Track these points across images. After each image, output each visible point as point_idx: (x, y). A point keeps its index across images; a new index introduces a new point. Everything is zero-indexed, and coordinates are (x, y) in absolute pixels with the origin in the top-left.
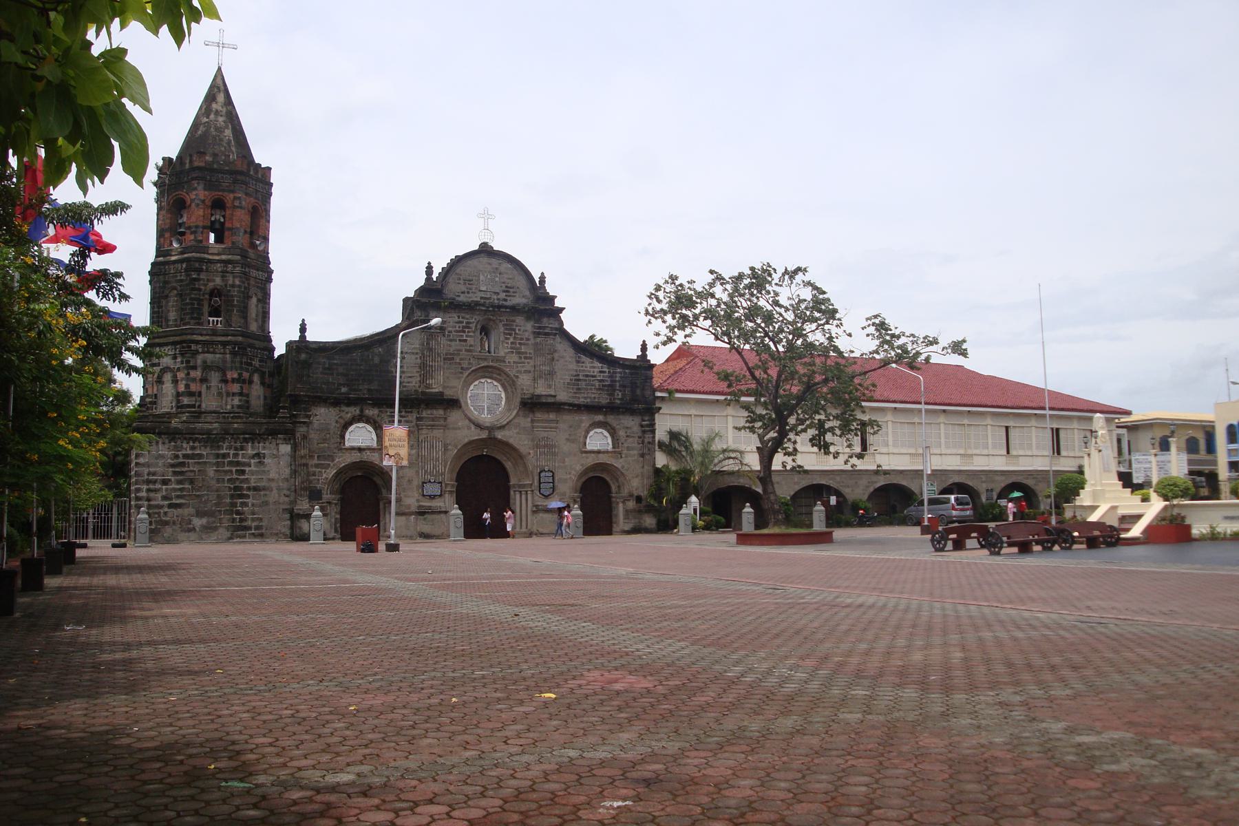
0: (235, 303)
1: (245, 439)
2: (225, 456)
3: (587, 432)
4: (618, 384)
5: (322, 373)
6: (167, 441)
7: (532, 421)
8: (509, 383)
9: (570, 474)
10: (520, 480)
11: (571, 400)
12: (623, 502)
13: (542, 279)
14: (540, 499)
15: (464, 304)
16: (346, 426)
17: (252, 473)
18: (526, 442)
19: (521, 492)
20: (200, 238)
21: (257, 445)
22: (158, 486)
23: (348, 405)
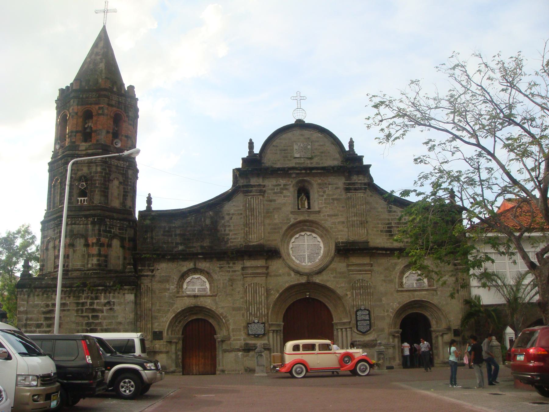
0: (97, 185)
1: (98, 290)
2: (83, 304)
3: (403, 273)
5: (163, 235)
6: (41, 294)
7: (348, 266)
8: (324, 232)
9: (387, 311)
10: (341, 319)
13: (351, 144)
14: (358, 336)
15: (279, 169)
16: (183, 276)
18: (343, 285)
19: (342, 329)
20: (74, 140)
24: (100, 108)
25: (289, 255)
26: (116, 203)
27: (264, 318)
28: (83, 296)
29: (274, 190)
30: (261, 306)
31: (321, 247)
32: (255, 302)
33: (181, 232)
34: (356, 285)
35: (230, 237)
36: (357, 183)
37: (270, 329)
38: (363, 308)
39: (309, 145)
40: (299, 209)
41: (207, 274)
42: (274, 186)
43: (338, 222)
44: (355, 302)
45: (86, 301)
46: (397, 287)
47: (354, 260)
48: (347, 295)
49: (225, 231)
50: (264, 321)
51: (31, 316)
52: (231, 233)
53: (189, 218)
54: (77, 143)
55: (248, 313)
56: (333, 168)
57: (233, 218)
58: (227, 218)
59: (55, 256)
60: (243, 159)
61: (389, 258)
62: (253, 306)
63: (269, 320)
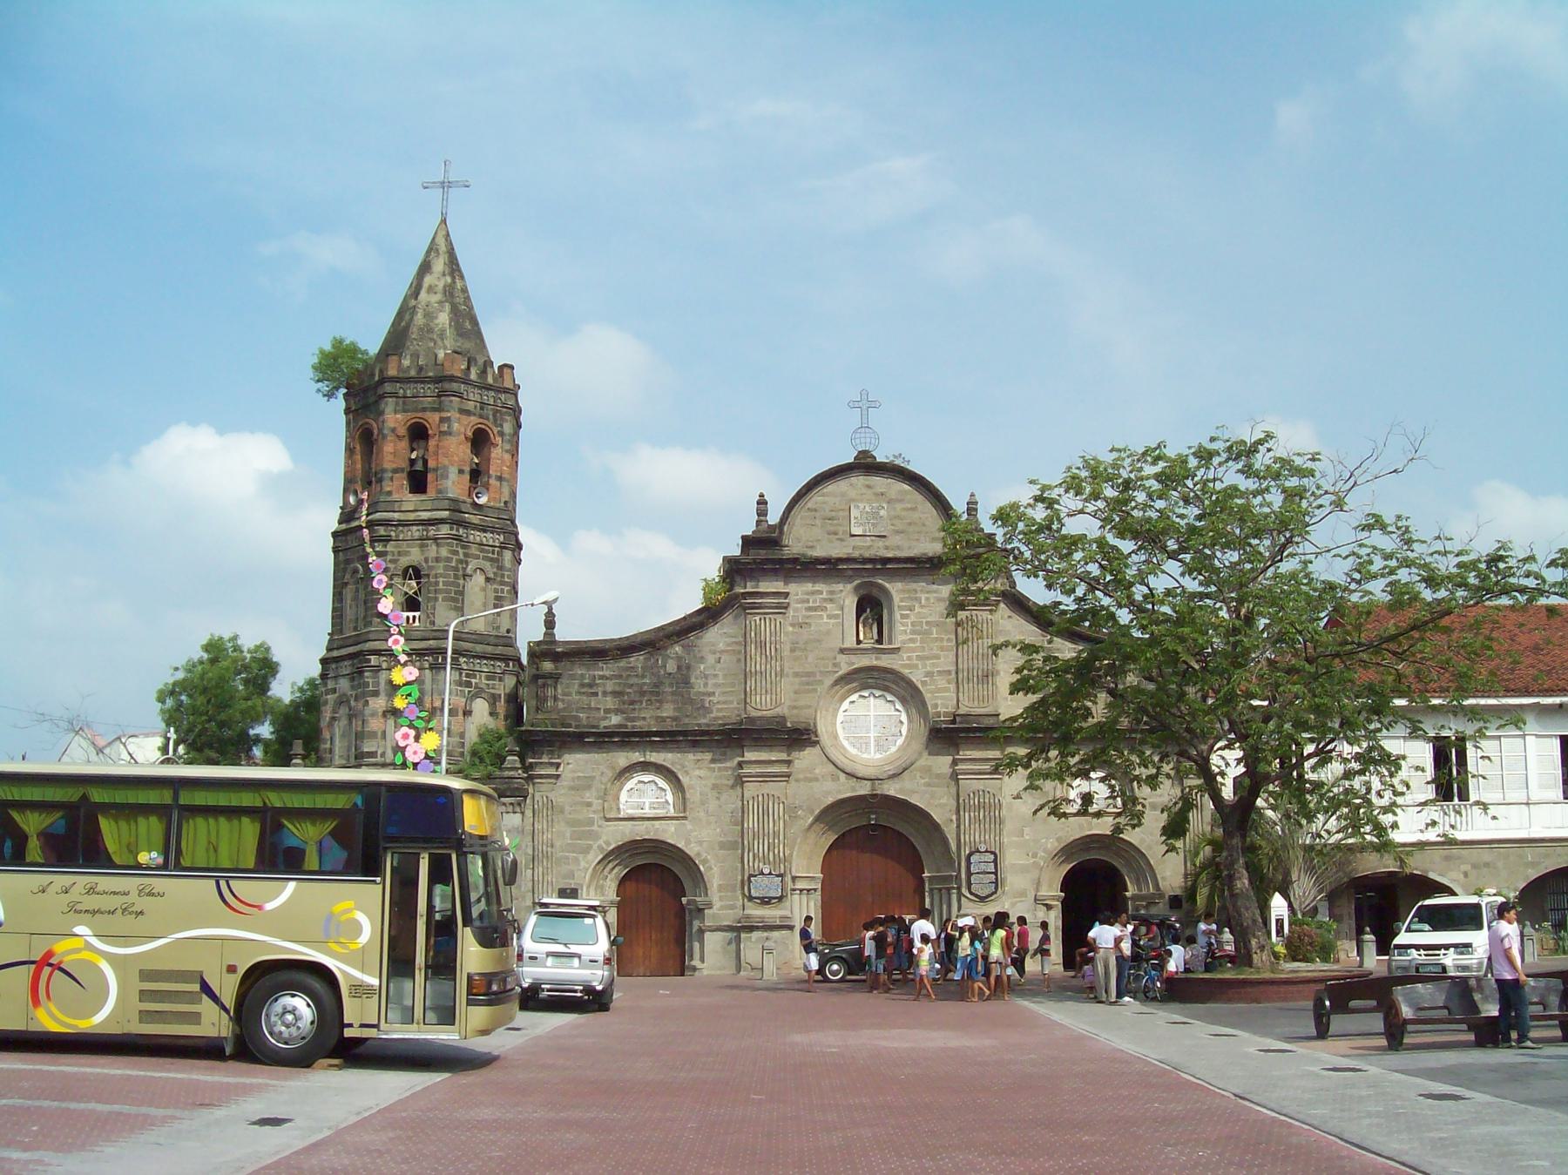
0: (441, 586)
7: (955, 762)
9: (1035, 855)
13: (972, 508)
18: (944, 801)
25: (836, 737)
29: (808, 602)
31: (901, 722)
33: (617, 689)
35: (715, 699)
42: (808, 594)
44: (967, 836)
49: (706, 685)
50: (782, 872)
53: (632, 659)
54: (395, 497)
55: (751, 854)
58: (711, 659)
60: (744, 538)
62: (761, 841)
63: (793, 870)
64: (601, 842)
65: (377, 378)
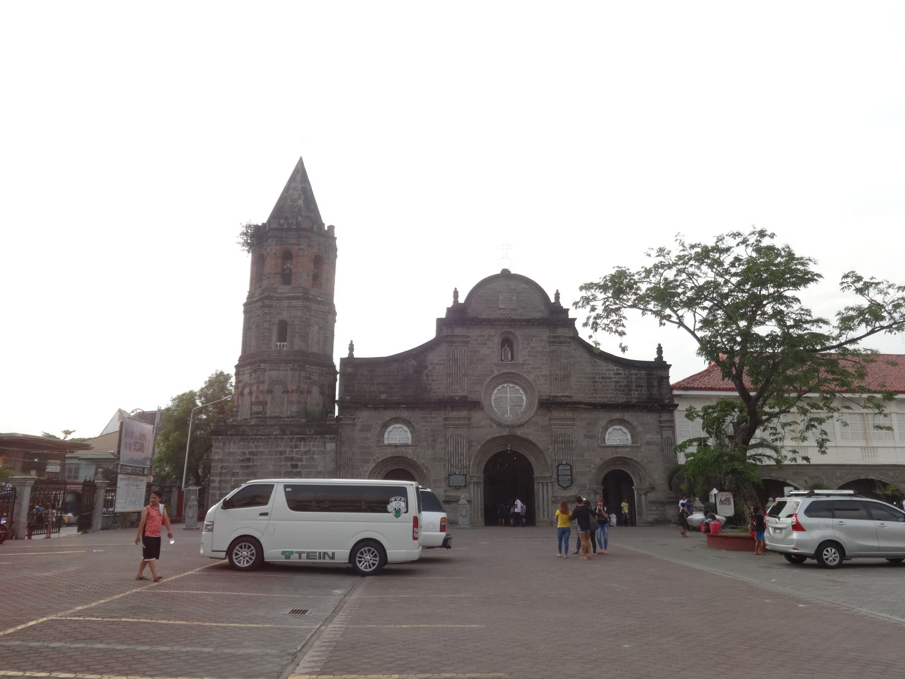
0: (297, 330)
2: (281, 453)
3: (606, 429)
4: (634, 384)
7: (550, 419)
8: (527, 386)
11: (589, 400)
12: (646, 494)
13: (557, 295)
15: (484, 320)
16: (385, 426)
17: (304, 467)
18: (545, 439)
21: (308, 443)
22: (228, 478)
23: (386, 408)
24: (300, 249)
25: (491, 406)
26: (315, 349)
27: (465, 470)
28: (282, 444)
29: (478, 340)
30: (462, 457)
31: (523, 400)
32: (457, 453)
34: (558, 440)
36: (562, 336)
37: (472, 481)
38: (564, 463)
39: (515, 296)
40: (502, 361)
41: (408, 423)
43: (541, 375)
45: (285, 449)
46: (600, 442)
47: (556, 414)
48: (548, 448)
49: (428, 380)
50: (465, 473)
51: (226, 464)
52: (433, 383)
55: (450, 464)
56: (538, 320)
57: (436, 368)
58: (430, 367)
59: (252, 403)
61: (593, 413)
62: (455, 457)
63: (470, 472)
64: (375, 457)
65: (267, 229)
